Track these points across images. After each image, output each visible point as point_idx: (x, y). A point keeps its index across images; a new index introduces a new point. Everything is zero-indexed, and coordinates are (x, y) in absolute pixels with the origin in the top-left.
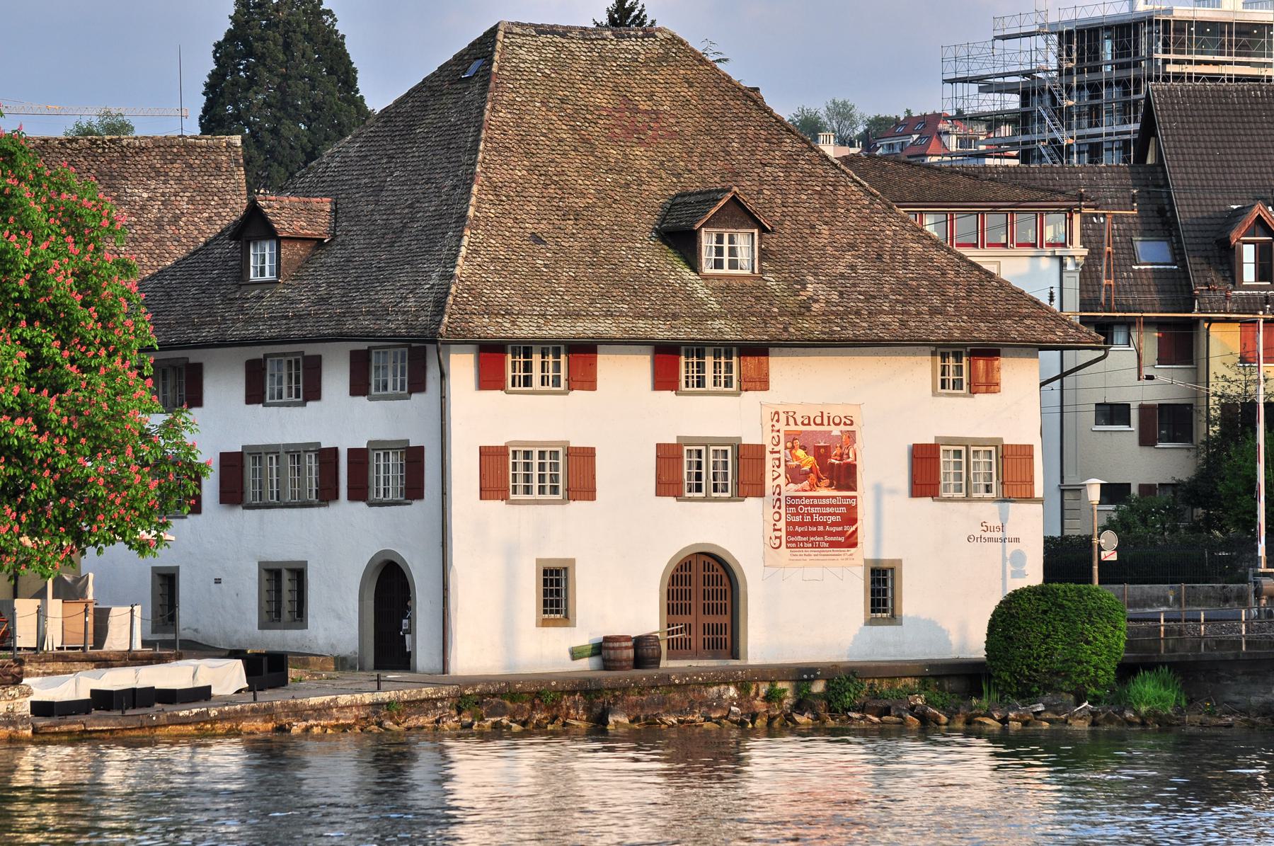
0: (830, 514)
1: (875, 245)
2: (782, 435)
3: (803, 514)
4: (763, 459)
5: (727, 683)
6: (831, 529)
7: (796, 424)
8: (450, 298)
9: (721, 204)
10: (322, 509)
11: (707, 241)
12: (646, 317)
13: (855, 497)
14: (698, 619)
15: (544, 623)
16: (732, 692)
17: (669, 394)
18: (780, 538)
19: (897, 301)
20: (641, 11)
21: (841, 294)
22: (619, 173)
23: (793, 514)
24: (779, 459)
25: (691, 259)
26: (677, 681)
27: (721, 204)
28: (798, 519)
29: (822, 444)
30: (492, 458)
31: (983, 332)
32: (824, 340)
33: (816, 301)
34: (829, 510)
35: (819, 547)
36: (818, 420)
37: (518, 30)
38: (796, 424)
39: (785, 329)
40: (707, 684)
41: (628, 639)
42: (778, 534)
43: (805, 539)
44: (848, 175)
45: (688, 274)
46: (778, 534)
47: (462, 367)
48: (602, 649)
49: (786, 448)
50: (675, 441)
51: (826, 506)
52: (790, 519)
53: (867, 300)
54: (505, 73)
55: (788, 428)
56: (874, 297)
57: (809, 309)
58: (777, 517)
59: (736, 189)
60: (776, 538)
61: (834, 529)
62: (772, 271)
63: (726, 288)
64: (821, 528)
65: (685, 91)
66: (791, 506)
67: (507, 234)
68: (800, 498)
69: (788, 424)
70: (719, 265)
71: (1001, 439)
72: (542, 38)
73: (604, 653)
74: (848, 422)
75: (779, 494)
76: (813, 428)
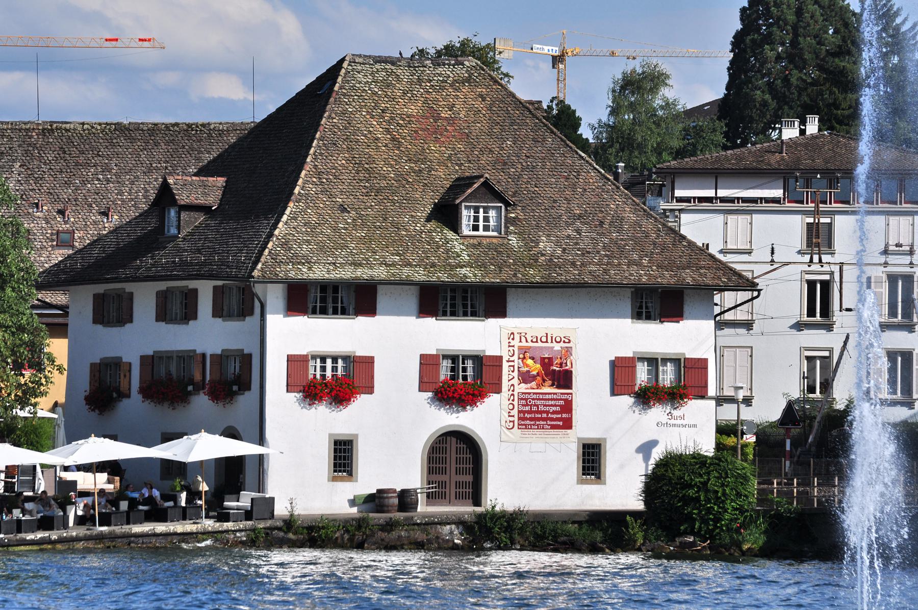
0: (552, 405)
1: (600, 215)
2: (516, 349)
3: (531, 405)
4: (501, 366)
6: (553, 416)
7: (527, 341)
8: (267, 250)
9: (476, 186)
12: (410, 265)
13: (571, 394)
14: (452, 477)
18: (513, 422)
19: (606, 255)
21: (564, 249)
22: (415, 162)
23: (523, 405)
24: (513, 366)
25: (455, 226)
26: (419, 521)
27: (476, 186)
28: (527, 408)
29: (546, 356)
30: (296, 363)
31: (667, 279)
33: (543, 255)
34: (551, 403)
35: (543, 428)
36: (544, 339)
37: (361, 60)
38: (527, 341)
40: (441, 523)
41: (394, 491)
42: (512, 419)
43: (532, 423)
44: (590, 164)
45: (450, 235)
46: (512, 419)
48: (376, 500)
49: (519, 358)
50: (435, 353)
51: (549, 400)
52: (522, 408)
53: (583, 254)
54: (344, 91)
55: (521, 344)
56: (589, 252)
57: (536, 261)
58: (511, 407)
59: (487, 175)
60: (510, 421)
61: (555, 416)
62: (516, 233)
63: (476, 245)
64: (544, 415)
65: (479, 104)
66: (522, 399)
67: (322, 206)
68: (529, 393)
69: (521, 341)
70: (476, 228)
71: (684, 354)
72: (378, 66)
73: (377, 501)
74: (567, 341)
75: (513, 391)
76: (540, 344)
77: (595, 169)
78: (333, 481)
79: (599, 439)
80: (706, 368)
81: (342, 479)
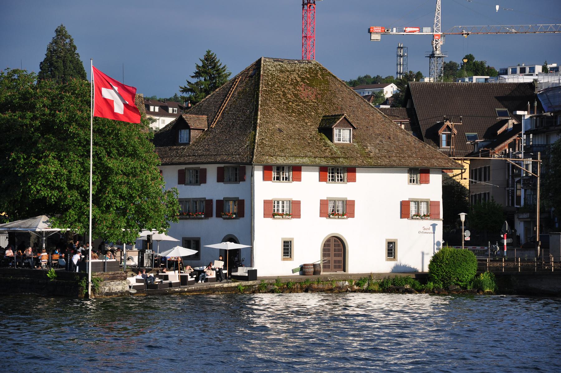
5: (345, 281)
10: (206, 220)
11: (336, 131)
15: (284, 259)
16: (347, 283)
17: (324, 183)
20: (215, 56)
21: (379, 150)
26: (330, 280)
30: (268, 204)
32: (376, 165)
39: (363, 162)
47: (258, 174)
48: (303, 269)
50: (326, 199)
56: (390, 151)
71: (430, 199)
72: (276, 63)
77: (379, 112)
78: (283, 260)
79: (395, 239)
80: (439, 206)
81: (287, 259)
